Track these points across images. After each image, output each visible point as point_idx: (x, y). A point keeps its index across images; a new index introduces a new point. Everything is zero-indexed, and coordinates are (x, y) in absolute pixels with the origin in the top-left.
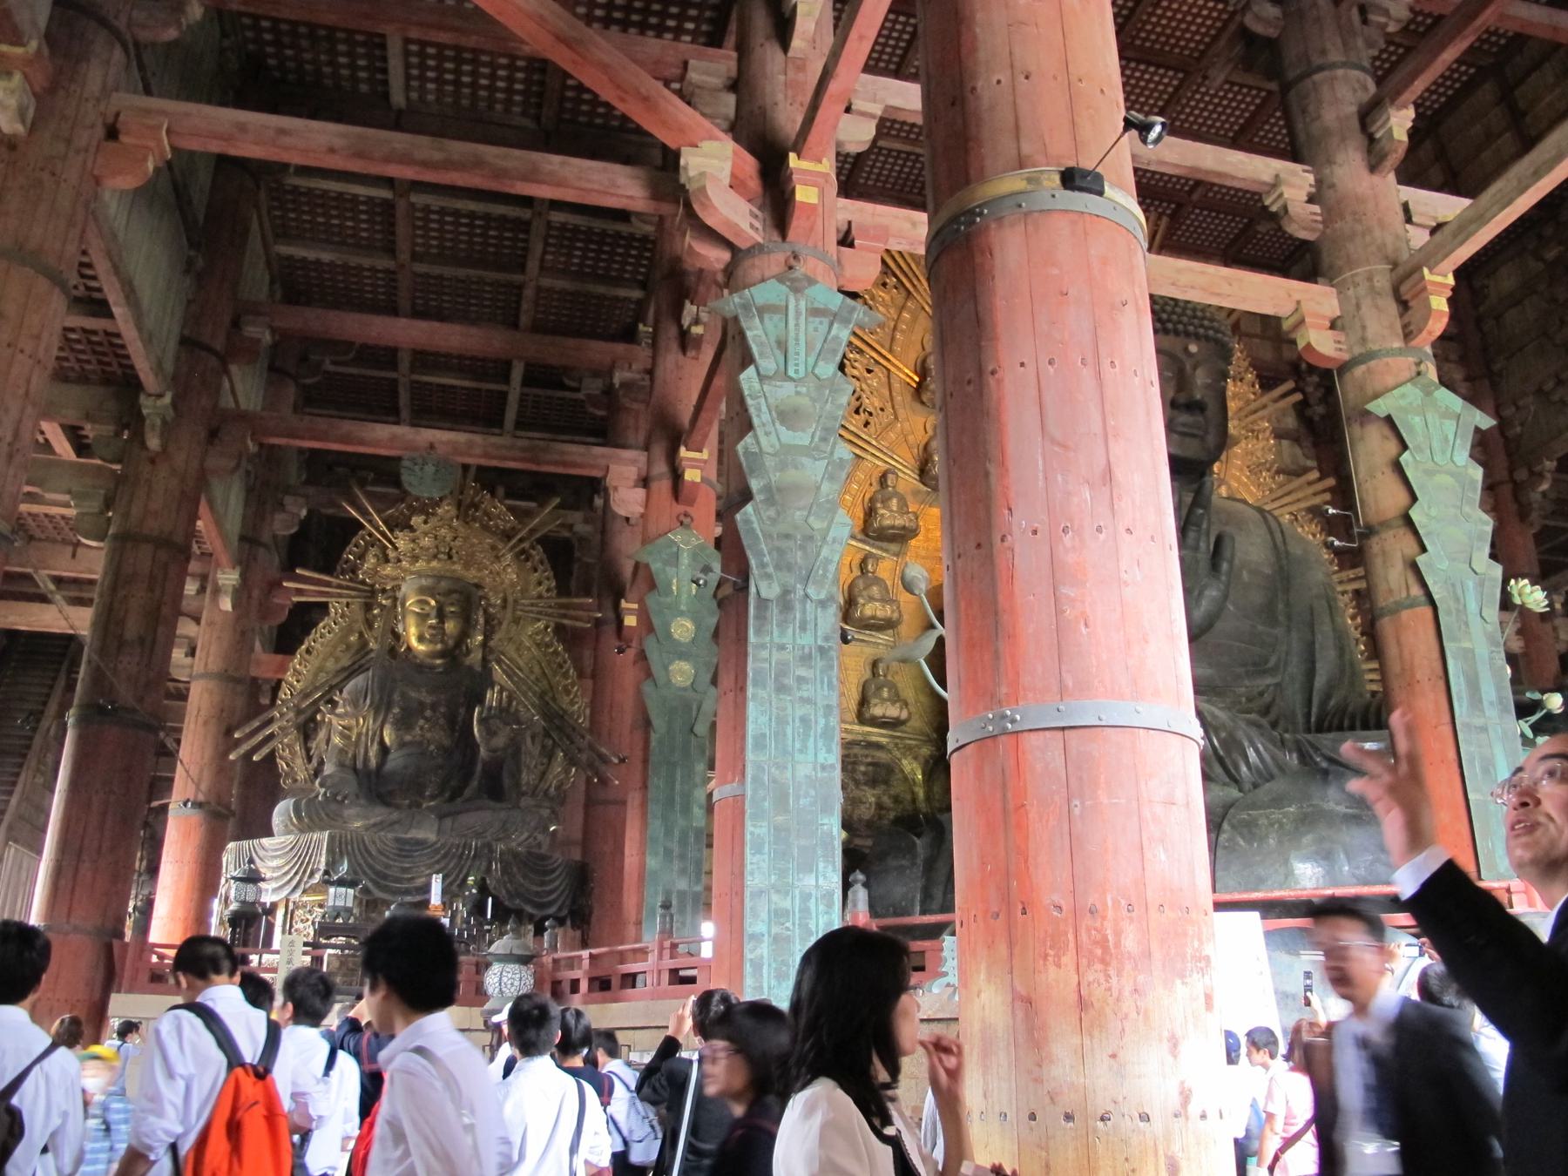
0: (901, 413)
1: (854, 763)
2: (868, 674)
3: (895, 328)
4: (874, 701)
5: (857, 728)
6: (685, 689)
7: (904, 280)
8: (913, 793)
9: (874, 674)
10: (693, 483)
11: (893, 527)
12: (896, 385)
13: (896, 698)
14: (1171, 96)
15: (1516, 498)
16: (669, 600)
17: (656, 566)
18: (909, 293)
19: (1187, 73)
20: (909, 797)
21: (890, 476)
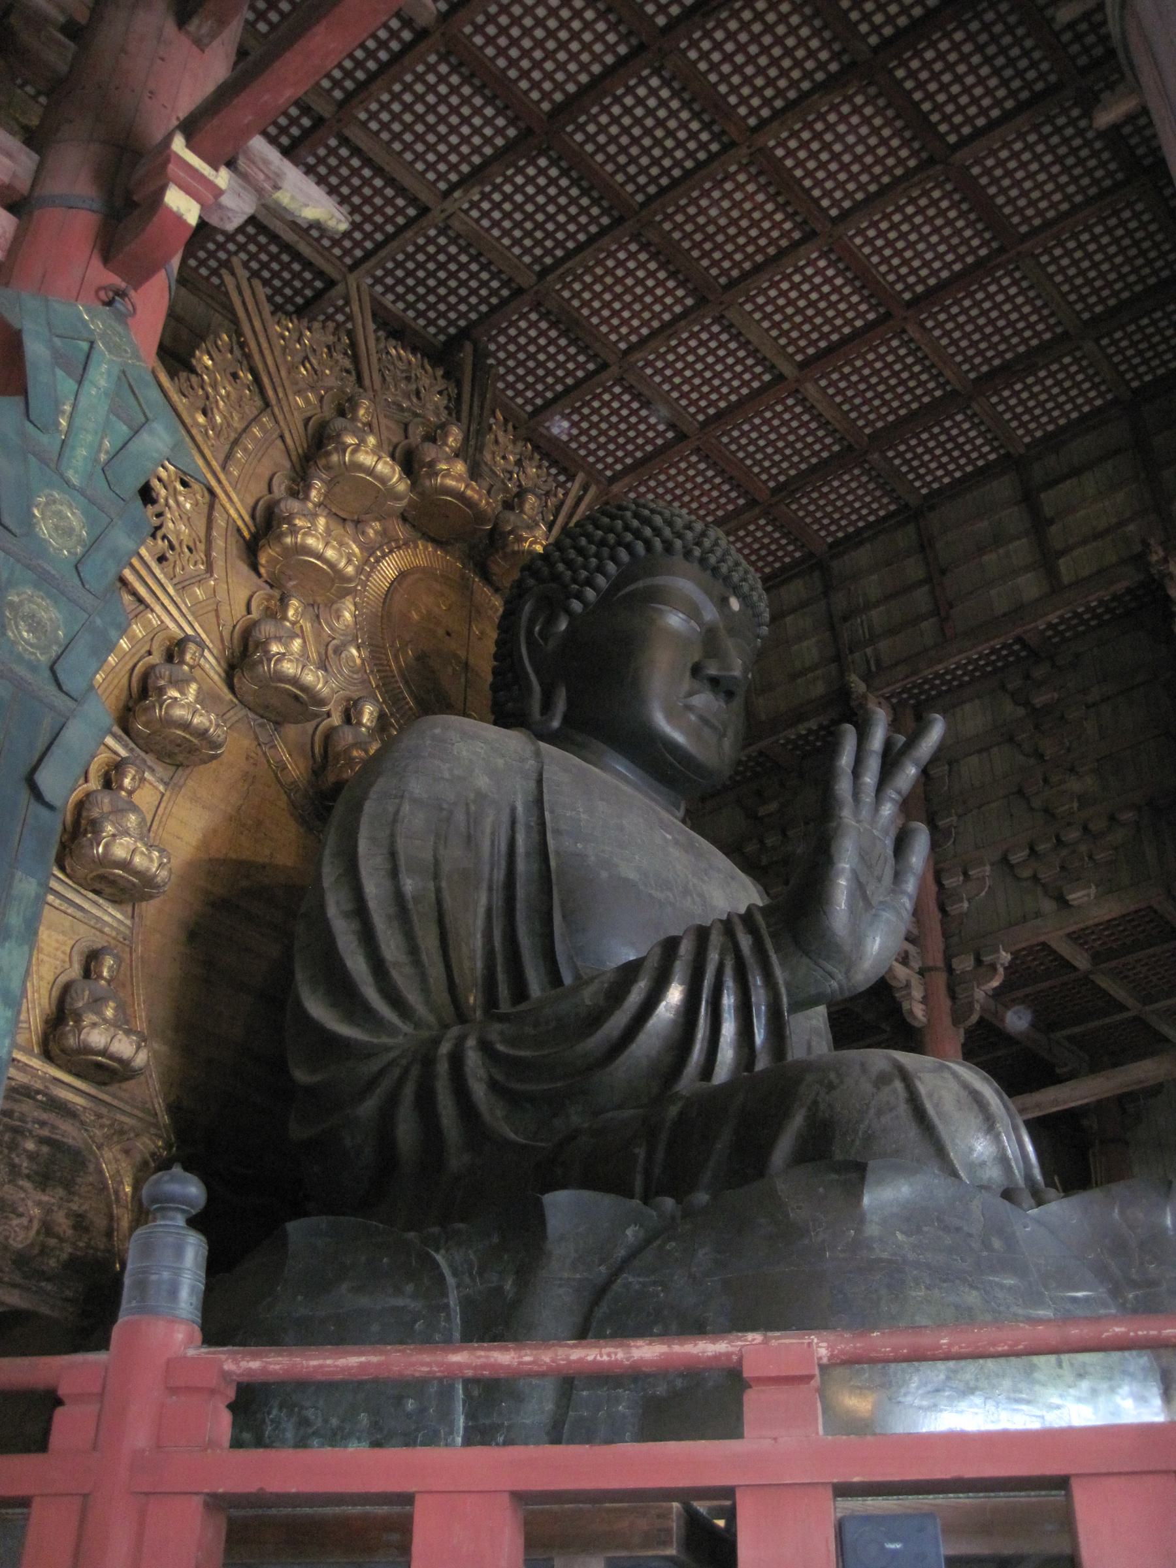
0: (219, 564)
1: (16, 1131)
2: (75, 971)
3: (236, 442)
4: (89, 1018)
5: (36, 1063)
6: (33, 668)
7: (266, 380)
8: (111, 1217)
9: (87, 973)
10: (179, 219)
11: (186, 726)
12: (220, 521)
13: (123, 1023)
14: (665, 326)
15: (953, 995)
16: (44, 439)
17: (36, 349)
18: (267, 404)
19: (702, 301)
20: (101, 1223)
21: (192, 647)
